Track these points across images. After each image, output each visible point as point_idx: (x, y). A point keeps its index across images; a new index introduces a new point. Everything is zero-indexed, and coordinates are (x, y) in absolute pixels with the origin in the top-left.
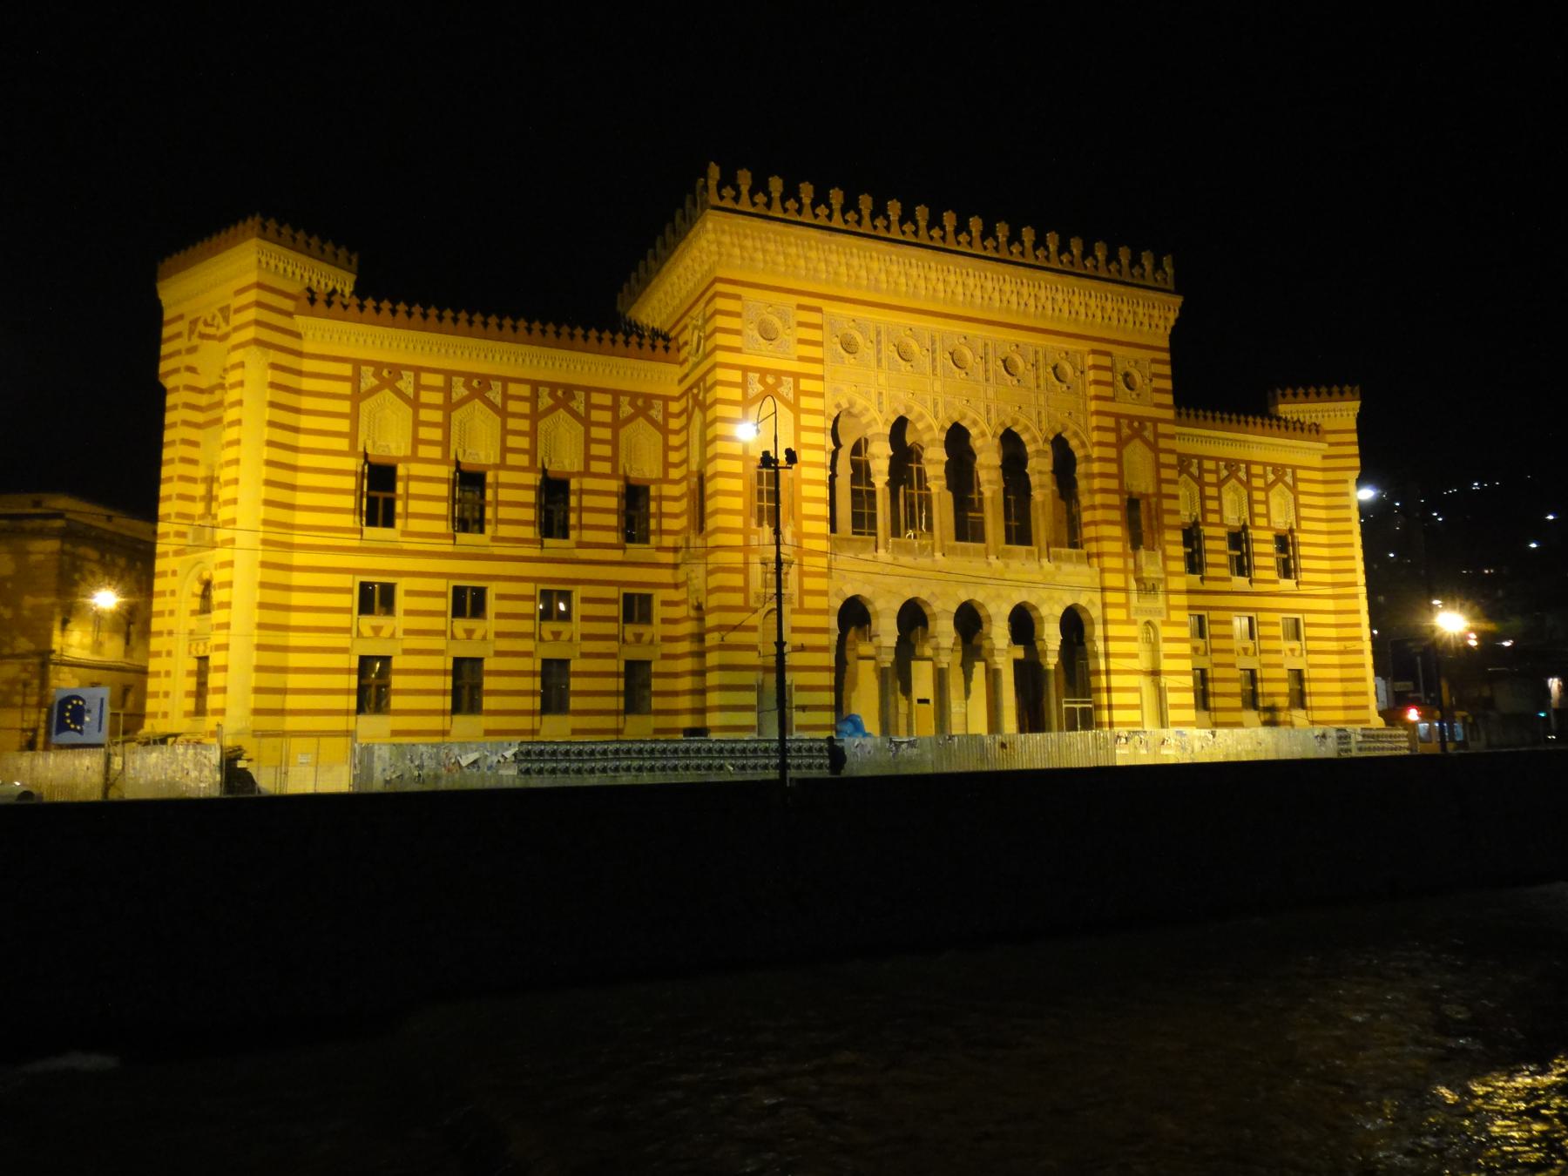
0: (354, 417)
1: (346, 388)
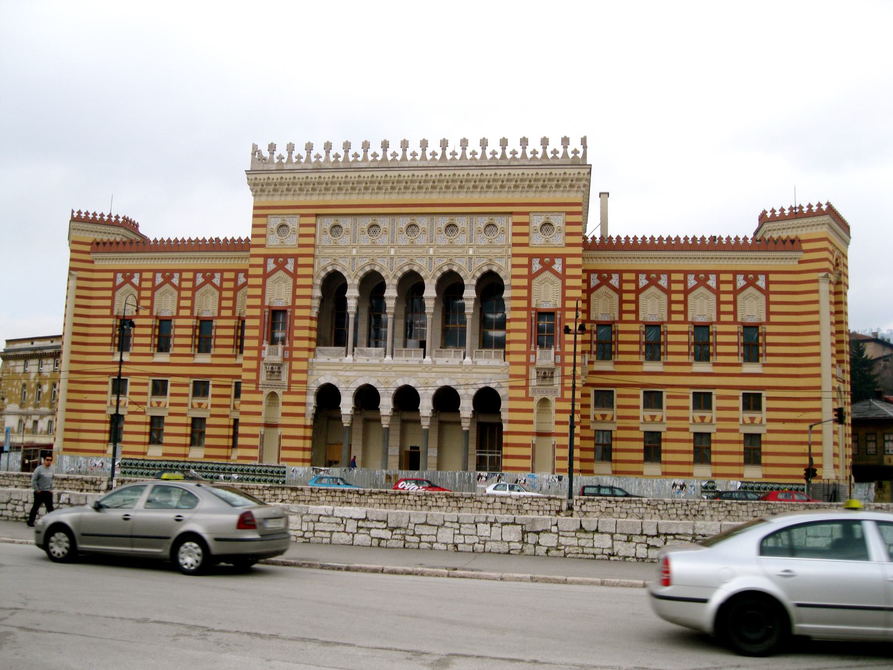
0: (112, 298)
1: (110, 284)
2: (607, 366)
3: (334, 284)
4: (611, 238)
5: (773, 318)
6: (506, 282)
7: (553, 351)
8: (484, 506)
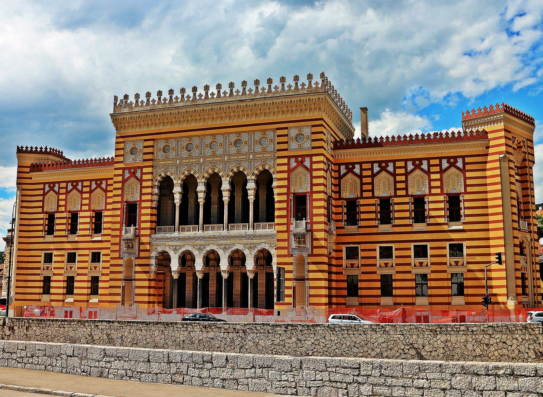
0: (43, 201)
1: (41, 192)
2: (353, 229)
3: (166, 184)
4: (370, 139)
5: (469, 189)
6: (274, 176)
7: (304, 222)
8: (223, 330)
